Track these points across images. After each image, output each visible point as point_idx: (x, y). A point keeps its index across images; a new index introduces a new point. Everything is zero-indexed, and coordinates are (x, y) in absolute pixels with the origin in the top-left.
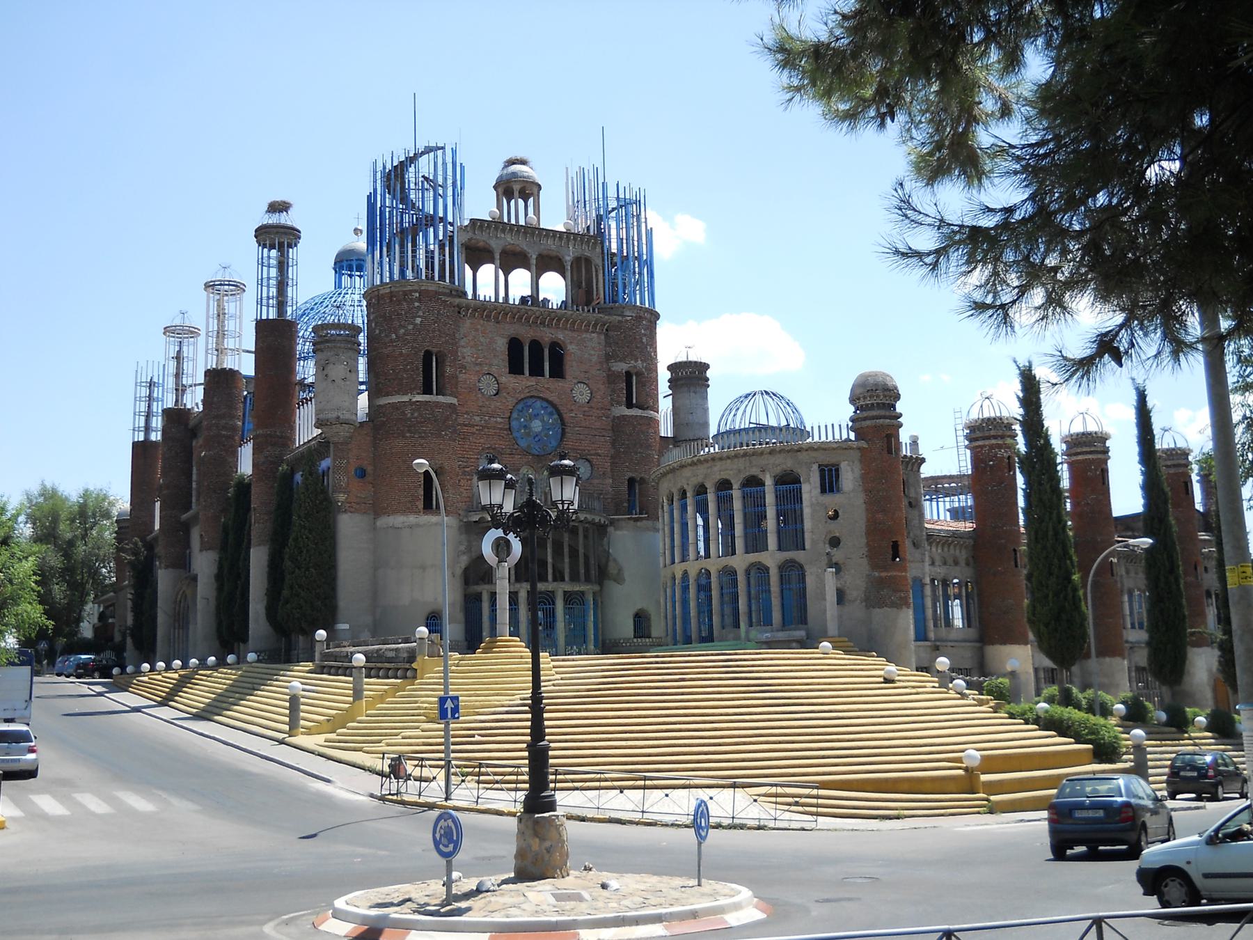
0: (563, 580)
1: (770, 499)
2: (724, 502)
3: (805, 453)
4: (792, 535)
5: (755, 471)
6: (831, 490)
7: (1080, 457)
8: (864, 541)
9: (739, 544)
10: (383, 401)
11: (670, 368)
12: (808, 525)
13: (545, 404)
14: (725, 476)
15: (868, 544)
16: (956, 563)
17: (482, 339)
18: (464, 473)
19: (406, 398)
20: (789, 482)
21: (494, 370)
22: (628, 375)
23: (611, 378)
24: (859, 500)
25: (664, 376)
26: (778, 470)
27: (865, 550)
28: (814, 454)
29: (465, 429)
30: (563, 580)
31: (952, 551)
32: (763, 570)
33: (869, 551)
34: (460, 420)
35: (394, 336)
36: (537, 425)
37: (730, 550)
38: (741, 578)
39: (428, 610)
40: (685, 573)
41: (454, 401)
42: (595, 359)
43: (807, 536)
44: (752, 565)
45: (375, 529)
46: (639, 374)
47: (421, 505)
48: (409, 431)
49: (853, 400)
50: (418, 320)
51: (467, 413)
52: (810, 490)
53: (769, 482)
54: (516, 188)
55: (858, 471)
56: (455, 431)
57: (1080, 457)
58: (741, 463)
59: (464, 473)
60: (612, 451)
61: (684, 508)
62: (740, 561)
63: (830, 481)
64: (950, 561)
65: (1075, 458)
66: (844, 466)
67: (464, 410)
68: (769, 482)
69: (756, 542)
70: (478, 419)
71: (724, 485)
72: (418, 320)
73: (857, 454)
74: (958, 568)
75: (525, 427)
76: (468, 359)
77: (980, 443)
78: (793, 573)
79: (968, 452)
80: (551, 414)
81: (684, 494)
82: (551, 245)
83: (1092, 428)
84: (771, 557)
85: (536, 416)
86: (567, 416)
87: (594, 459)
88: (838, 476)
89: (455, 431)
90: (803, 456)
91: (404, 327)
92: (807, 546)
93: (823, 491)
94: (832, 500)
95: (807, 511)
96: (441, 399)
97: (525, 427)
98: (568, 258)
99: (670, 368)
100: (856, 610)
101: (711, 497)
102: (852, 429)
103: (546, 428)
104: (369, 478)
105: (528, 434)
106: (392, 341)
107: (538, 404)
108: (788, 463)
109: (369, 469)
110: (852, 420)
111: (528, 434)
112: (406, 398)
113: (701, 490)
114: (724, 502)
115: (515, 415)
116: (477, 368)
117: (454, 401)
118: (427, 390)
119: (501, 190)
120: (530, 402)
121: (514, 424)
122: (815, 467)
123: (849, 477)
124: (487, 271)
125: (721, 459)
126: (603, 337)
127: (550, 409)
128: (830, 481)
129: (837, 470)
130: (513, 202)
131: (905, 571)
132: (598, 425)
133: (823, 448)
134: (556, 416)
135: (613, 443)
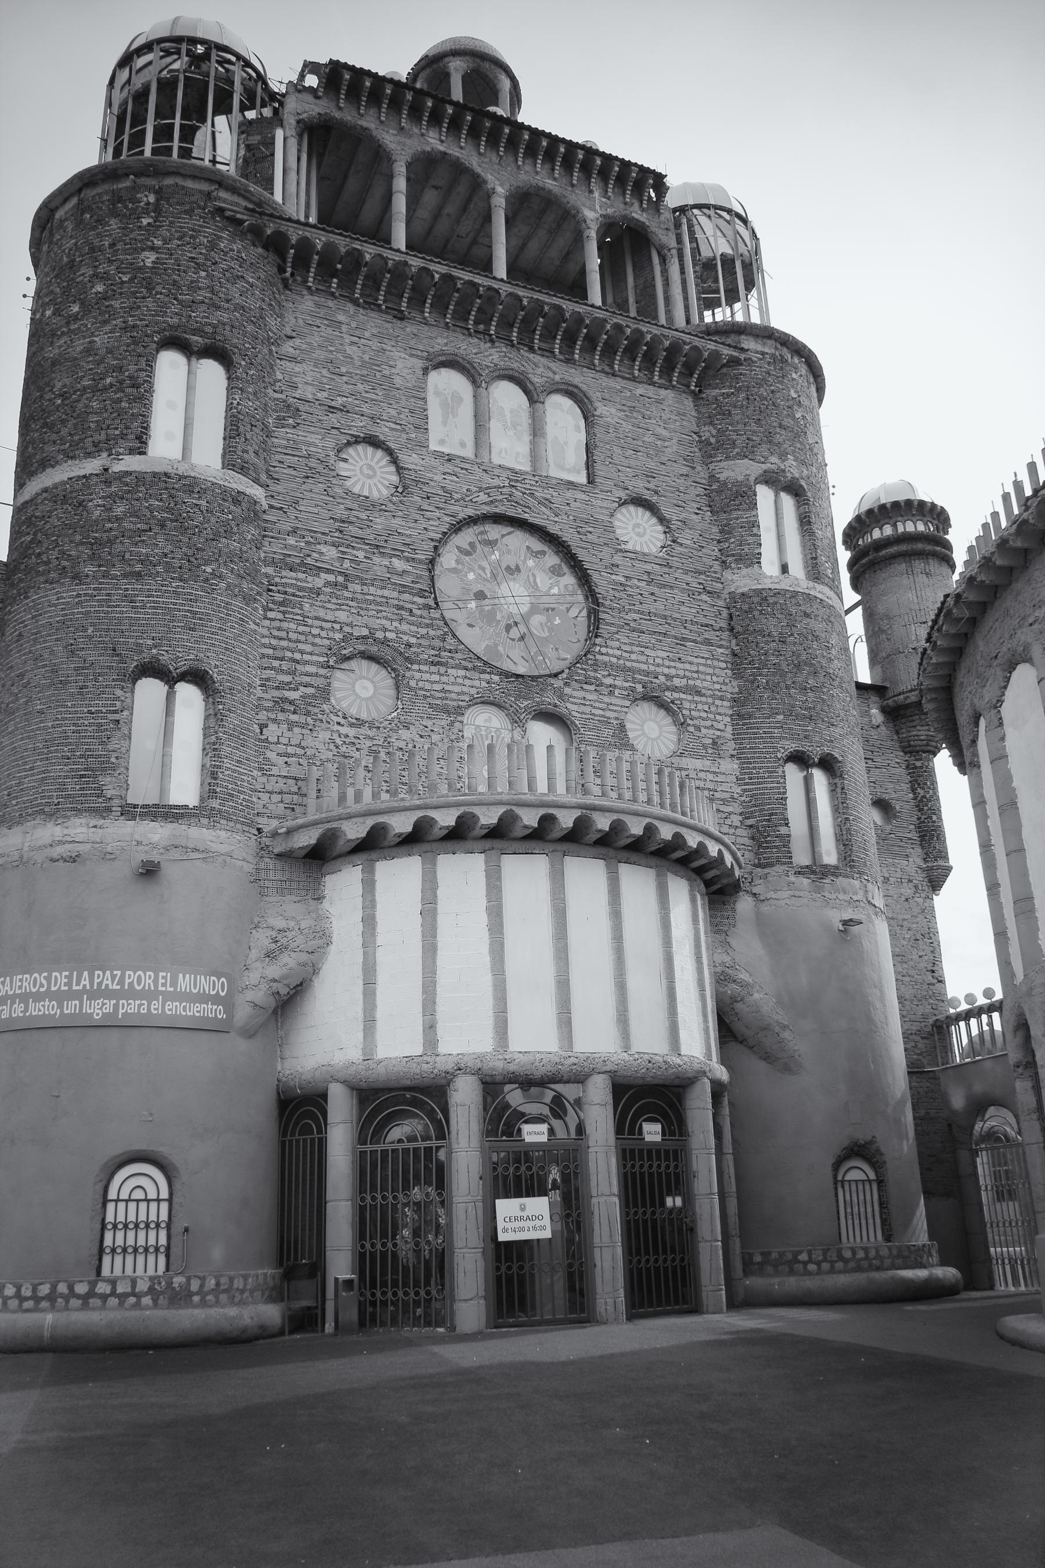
10: (34, 486)
13: (537, 545)
17: (350, 350)
18: (281, 704)
19: (91, 466)
21: (383, 431)
29: (289, 577)
34: (273, 548)
35: (76, 308)
36: (514, 597)
41: (257, 492)
42: (672, 448)
48: (92, 557)
50: (149, 258)
51: (294, 531)
54: (457, 68)
56: (252, 574)
59: (281, 704)
60: (733, 687)
70: (330, 552)
72: (149, 258)
75: (480, 596)
76: (308, 392)
80: (555, 571)
85: (514, 571)
86: (601, 582)
89: (252, 574)
91: (104, 277)
97: (480, 596)
98: (589, 215)
105: (490, 617)
107: (518, 541)
111: (490, 617)
112: (91, 466)
115: (448, 559)
116: (334, 419)
117: (257, 492)
120: (494, 531)
121: (446, 584)
126: (688, 403)
127: (552, 559)
132: (688, 612)
134: (569, 580)
135: (737, 662)
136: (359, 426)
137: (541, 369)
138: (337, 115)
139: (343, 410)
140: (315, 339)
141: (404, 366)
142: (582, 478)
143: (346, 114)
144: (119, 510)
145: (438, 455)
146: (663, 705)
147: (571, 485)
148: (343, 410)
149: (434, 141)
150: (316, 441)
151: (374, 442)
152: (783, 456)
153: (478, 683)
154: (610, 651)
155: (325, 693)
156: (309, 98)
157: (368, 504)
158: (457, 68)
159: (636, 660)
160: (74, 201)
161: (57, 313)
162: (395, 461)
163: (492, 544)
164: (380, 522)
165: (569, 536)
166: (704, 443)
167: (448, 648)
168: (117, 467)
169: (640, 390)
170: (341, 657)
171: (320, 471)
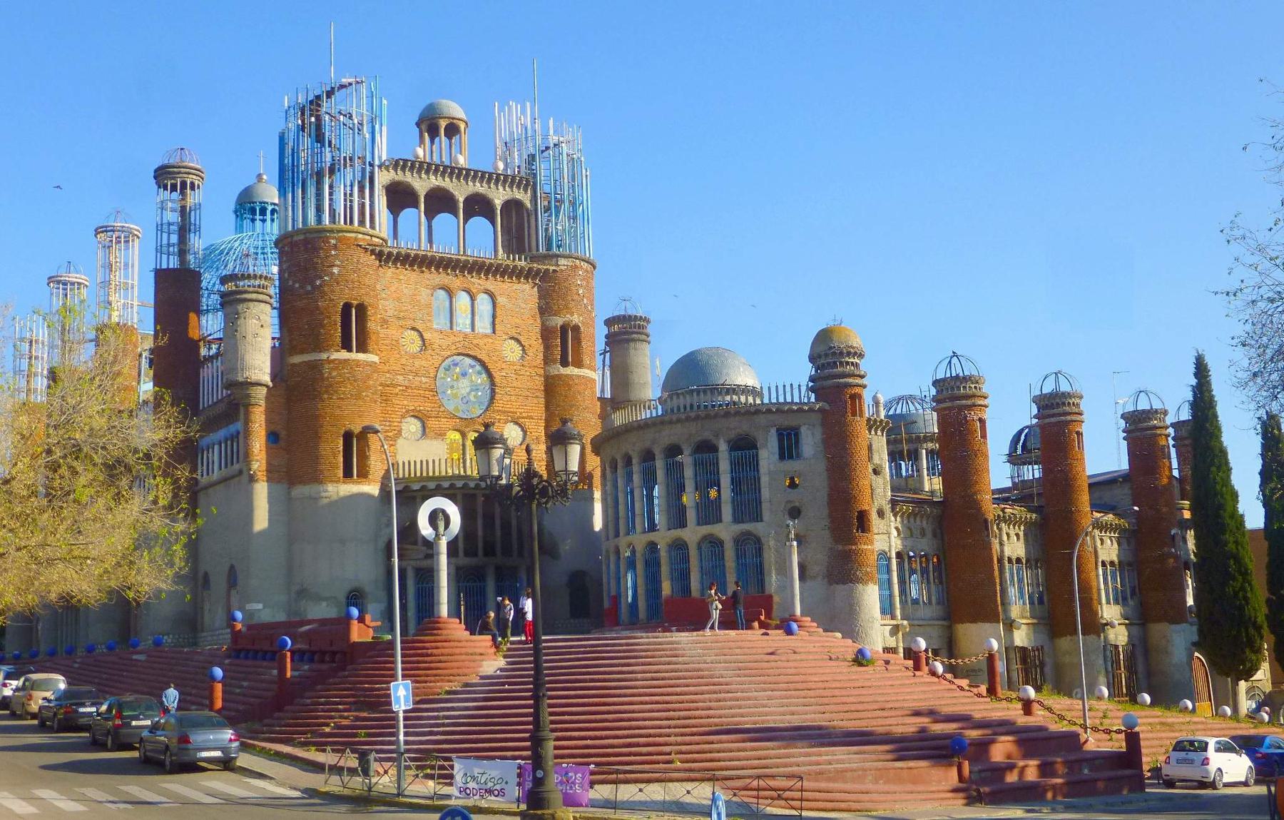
0: (494, 554)
1: (724, 466)
2: (675, 472)
3: (762, 416)
4: (748, 507)
5: (707, 435)
6: (791, 457)
7: (1053, 420)
8: (826, 512)
9: (691, 515)
11: (608, 322)
12: (765, 493)
14: (674, 439)
15: (830, 516)
16: (923, 534)
17: (406, 291)
20: (745, 447)
21: (419, 326)
22: (564, 329)
23: (546, 334)
24: (821, 466)
25: (601, 332)
26: (732, 435)
27: (826, 522)
28: (770, 417)
30: (494, 554)
31: (918, 522)
32: (714, 543)
33: (832, 522)
35: (309, 288)
36: (464, 386)
37: (682, 524)
38: (693, 553)
39: (347, 587)
40: (652, 546)
43: (765, 506)
44: (705, 538)
45: (289, 499)
46: (576, 329)
47: (340, 473)
49: (812, 359)
52: (768, 456)
53: (723, 447)
54: (443, 124)
55: (818, 432)
57: (1053, 420)
58: (693, 428)
61: (629, 476)
62: (692, 533)
63: (789, 445)
64: (917, 532)
65: (1047, 421)
66: (803, 430)
67: (386, 368)
68: (723, 447)
69: (709, 513)
70: (401, 378)
71: (673, 451)
72: (335, 270)
73: (816, 418)
74: (924, 541)
76: (390, 313)
77: (948, 404)
78: (750, 547)
79: (935, 414)
80: (479, 373)
81: (628, 461)
82: (479, 188)
83: (1065, 387)
84: (726, 530)
85: (464, 374)
86: (497, 375)
87: (527, 423)
88: (797, 442)
90: (762, 419)
92: (765, 518)
93: (782, 457)
94: (790, 465)
95: (764, 480)
96: (361, 356)
99: (608, 322)
100: (818, 585)
101: (660, 464)
102: (812, 390)
103: (475, 388)
104: (282, 443)
106: (308, 293)
108: (743, 427)
109: (283, 434)
110: (812, 379)
113: (648, 456)
114: (675, 472)
115: (441, 374)
117: (375, 358)
118: (347, 346)
119: (423, 127)
122: (773, 431)
123: (810, 441)
124: (412, 217)
125: (671, 422)
127: (478, 368)
128: (789, 445)
129: (797, 435)
130: (437, 140)
131: (872, 543)
133: (780, 410)
134: (484, 376)
135: (547, 407)
136: (409, 323)
137: (477, 282)
138: (397, 178)
139: (404, 318)
140: (393, 289)
141: (424, 293)
142: (489, 331)
143: (399, 176)
144: (334, 374)
145: (436, 331)
146: (517, 423)
147: (486, 336)
148: (404, 318)
149: (435, 181)
150: (393, 332)
151: (413, 329)
152: (572, 314)
153: (451, 423)
154: (498, 405)
155: (400, 432)
156: (385, 172)
157: (414, 356)
158: (443, 124)
159: (508, 407)
160: (302, 237)
161: (301, 287)
162: (421, 336)
163: (456, 365)
164: (417, 363)
165: (486, 359)
166: (540, 308)
167: (442, 413)
168: (332, 357)
169: (516, 286)
170: (403, 417)
171: (395, 345)
